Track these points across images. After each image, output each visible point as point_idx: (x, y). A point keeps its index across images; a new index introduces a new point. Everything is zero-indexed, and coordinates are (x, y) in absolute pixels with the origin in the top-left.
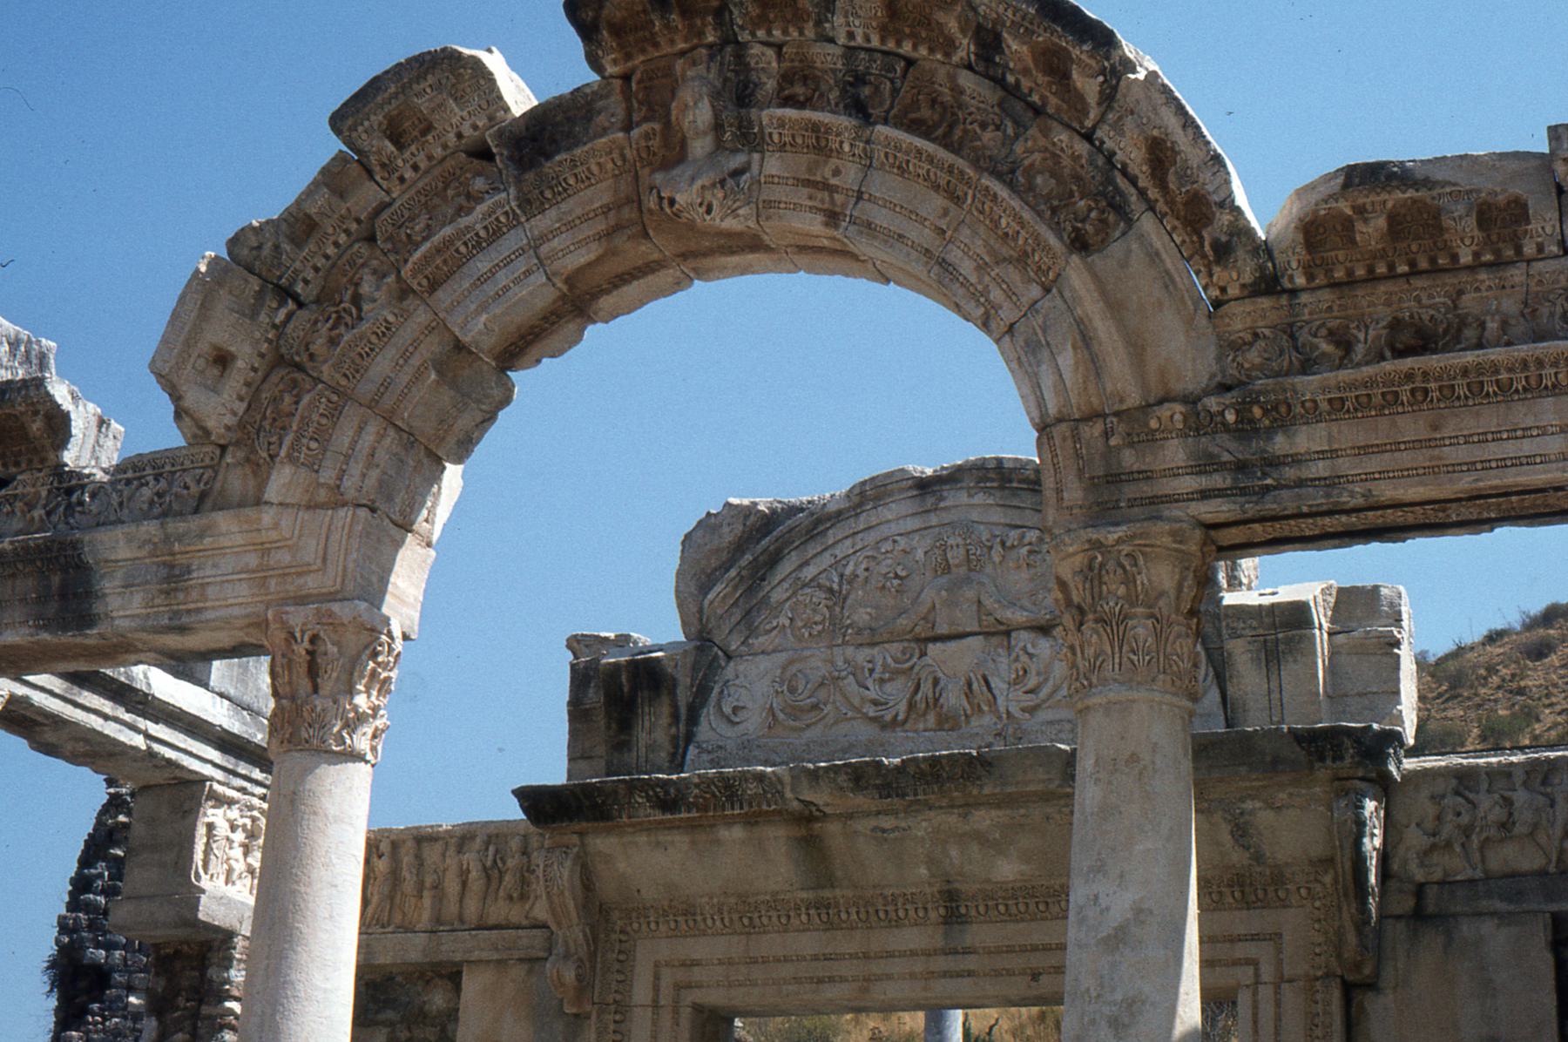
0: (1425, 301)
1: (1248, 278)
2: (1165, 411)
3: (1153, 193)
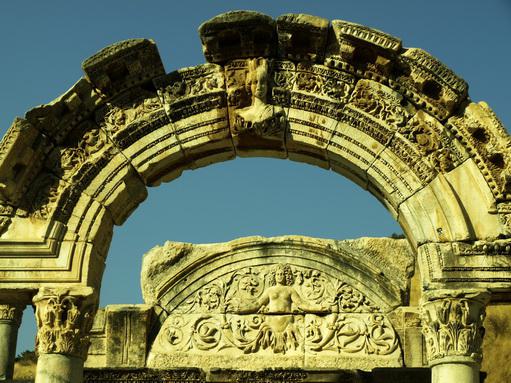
3: (474, 151)
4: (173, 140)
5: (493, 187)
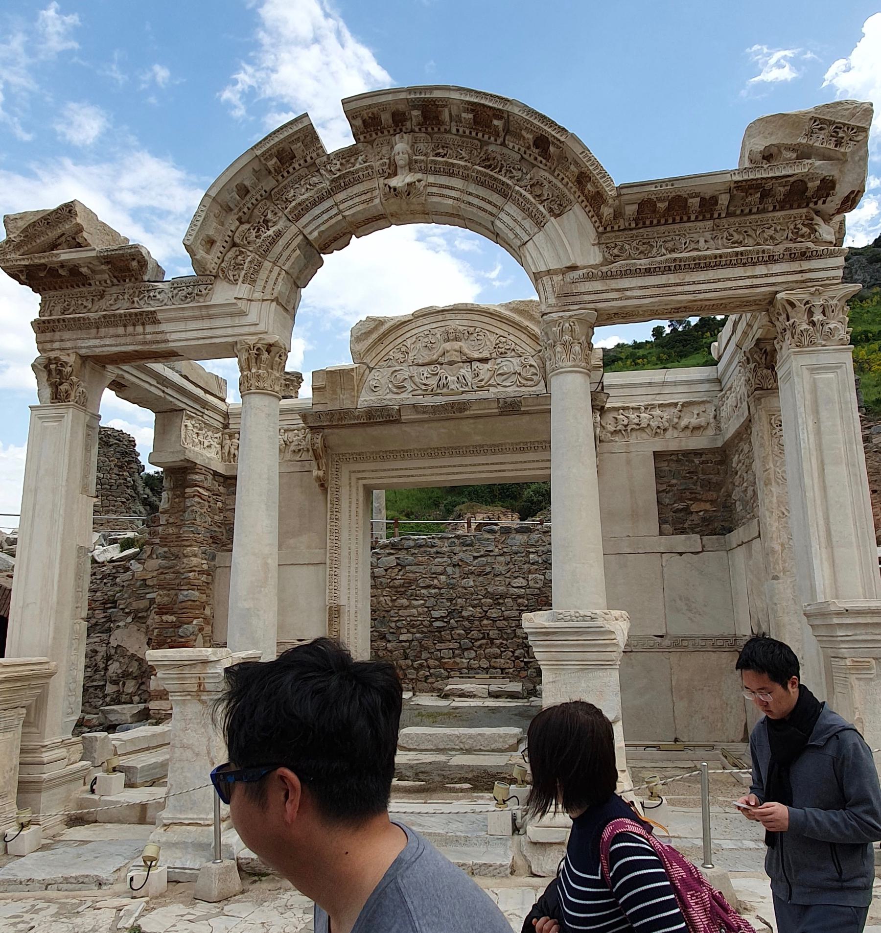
4: (334, 211)
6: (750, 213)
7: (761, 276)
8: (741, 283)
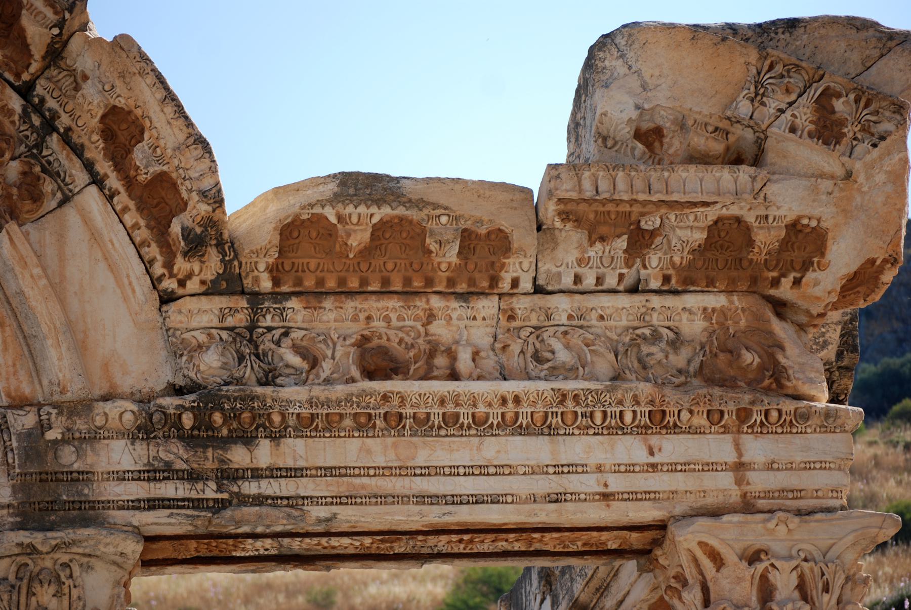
0: (394, 322)
1: (209, 276)
2: (112, 409)
3: (104, 167)
5: (152, 262)
6: (601, 288)
7: (630, 469)
8: (573, 483)
